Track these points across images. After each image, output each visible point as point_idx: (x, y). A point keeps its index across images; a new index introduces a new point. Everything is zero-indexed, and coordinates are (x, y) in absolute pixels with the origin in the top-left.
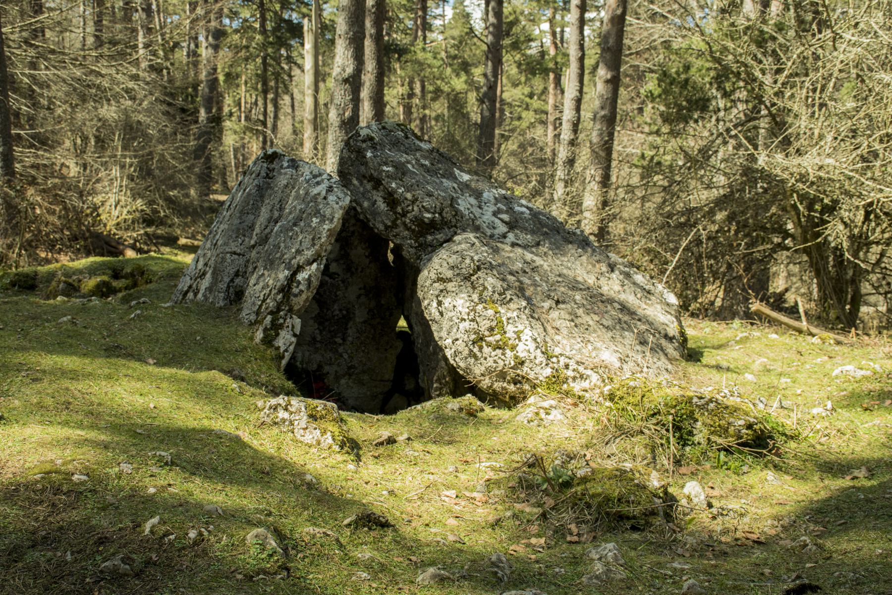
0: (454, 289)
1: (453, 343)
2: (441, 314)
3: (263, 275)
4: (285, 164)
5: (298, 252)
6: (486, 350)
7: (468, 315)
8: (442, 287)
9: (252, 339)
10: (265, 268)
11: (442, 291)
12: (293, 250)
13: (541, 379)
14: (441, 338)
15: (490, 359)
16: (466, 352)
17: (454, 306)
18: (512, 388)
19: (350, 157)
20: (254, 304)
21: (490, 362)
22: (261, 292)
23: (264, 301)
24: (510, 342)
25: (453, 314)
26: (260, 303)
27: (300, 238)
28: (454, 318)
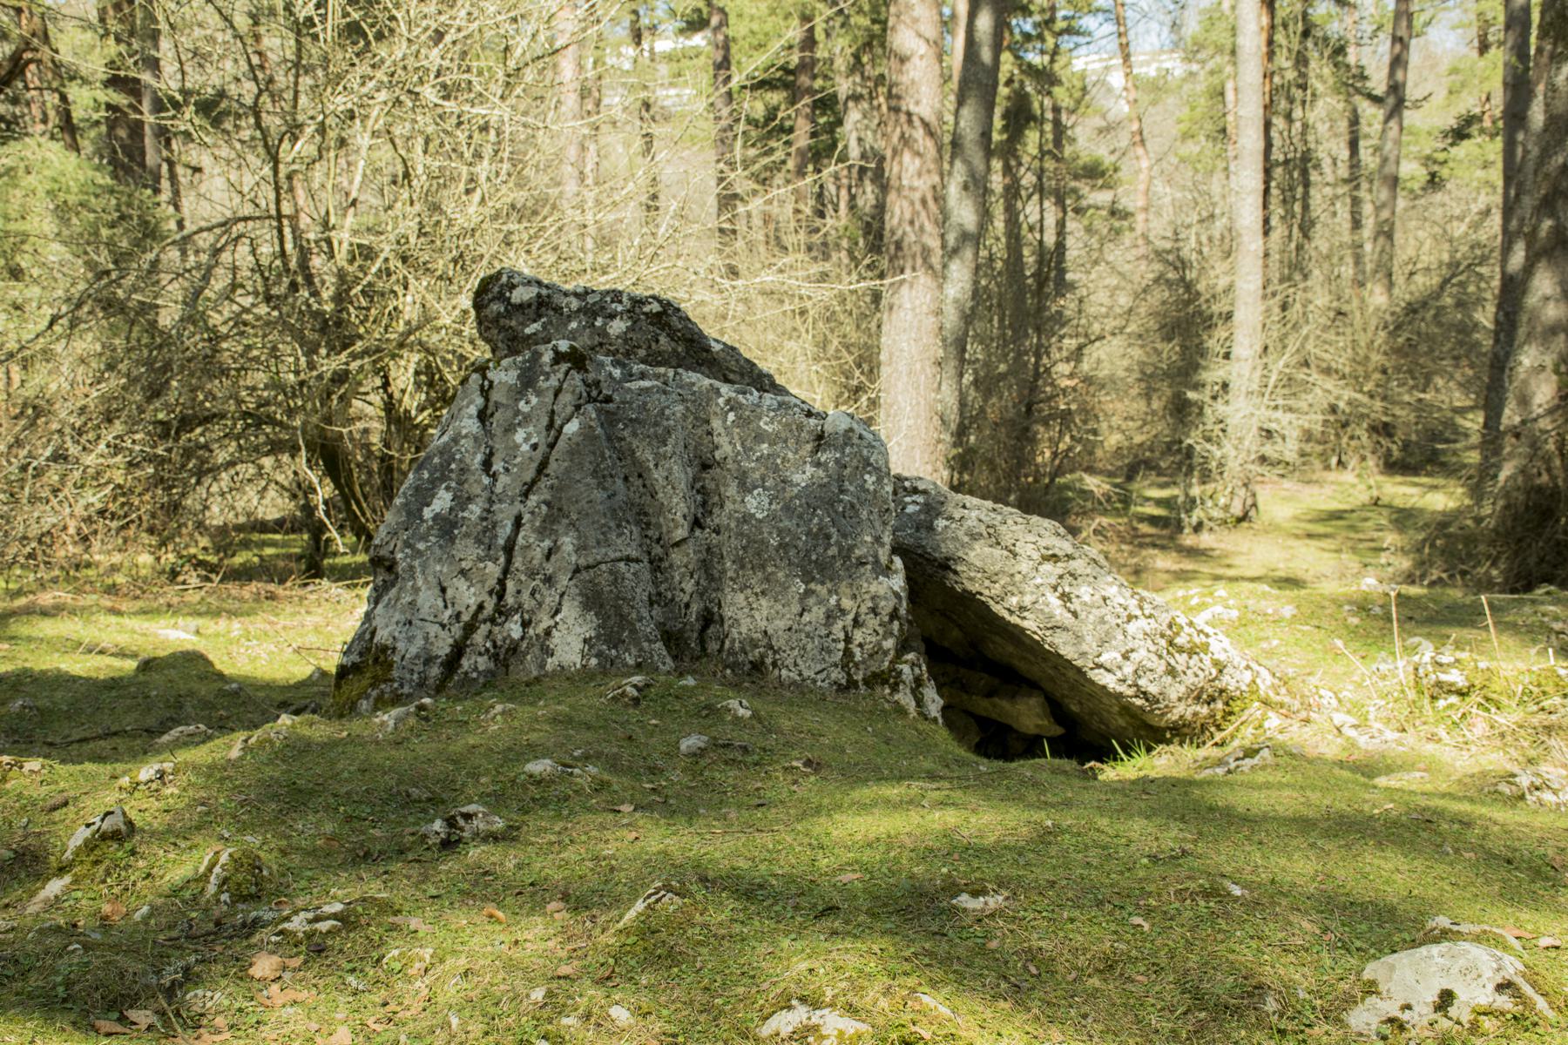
0: (1088, 571)
1: (1126, 657)
2: (1075, 614)
3: (809, 593)
4: (617, 373)
5: (878, 540)
6: (1182, 658)
7: (1141, 608)
8: (1061, 571)
9: (901, 711)
10: (808, 578)
11: (1061, 577)
12: (868, 539)
13: (1244, 688)
14: (1083, 654)
15: (1196, 672)
16: (1161, 667)
18: (1204, 710)
19: (674, 350)
21: (1190, 679)
23: (848, 640)
24: (1197, 640)
25: (1103, 611)
26: (841, 645)
27: (864, 514)
28: (1108, 618)
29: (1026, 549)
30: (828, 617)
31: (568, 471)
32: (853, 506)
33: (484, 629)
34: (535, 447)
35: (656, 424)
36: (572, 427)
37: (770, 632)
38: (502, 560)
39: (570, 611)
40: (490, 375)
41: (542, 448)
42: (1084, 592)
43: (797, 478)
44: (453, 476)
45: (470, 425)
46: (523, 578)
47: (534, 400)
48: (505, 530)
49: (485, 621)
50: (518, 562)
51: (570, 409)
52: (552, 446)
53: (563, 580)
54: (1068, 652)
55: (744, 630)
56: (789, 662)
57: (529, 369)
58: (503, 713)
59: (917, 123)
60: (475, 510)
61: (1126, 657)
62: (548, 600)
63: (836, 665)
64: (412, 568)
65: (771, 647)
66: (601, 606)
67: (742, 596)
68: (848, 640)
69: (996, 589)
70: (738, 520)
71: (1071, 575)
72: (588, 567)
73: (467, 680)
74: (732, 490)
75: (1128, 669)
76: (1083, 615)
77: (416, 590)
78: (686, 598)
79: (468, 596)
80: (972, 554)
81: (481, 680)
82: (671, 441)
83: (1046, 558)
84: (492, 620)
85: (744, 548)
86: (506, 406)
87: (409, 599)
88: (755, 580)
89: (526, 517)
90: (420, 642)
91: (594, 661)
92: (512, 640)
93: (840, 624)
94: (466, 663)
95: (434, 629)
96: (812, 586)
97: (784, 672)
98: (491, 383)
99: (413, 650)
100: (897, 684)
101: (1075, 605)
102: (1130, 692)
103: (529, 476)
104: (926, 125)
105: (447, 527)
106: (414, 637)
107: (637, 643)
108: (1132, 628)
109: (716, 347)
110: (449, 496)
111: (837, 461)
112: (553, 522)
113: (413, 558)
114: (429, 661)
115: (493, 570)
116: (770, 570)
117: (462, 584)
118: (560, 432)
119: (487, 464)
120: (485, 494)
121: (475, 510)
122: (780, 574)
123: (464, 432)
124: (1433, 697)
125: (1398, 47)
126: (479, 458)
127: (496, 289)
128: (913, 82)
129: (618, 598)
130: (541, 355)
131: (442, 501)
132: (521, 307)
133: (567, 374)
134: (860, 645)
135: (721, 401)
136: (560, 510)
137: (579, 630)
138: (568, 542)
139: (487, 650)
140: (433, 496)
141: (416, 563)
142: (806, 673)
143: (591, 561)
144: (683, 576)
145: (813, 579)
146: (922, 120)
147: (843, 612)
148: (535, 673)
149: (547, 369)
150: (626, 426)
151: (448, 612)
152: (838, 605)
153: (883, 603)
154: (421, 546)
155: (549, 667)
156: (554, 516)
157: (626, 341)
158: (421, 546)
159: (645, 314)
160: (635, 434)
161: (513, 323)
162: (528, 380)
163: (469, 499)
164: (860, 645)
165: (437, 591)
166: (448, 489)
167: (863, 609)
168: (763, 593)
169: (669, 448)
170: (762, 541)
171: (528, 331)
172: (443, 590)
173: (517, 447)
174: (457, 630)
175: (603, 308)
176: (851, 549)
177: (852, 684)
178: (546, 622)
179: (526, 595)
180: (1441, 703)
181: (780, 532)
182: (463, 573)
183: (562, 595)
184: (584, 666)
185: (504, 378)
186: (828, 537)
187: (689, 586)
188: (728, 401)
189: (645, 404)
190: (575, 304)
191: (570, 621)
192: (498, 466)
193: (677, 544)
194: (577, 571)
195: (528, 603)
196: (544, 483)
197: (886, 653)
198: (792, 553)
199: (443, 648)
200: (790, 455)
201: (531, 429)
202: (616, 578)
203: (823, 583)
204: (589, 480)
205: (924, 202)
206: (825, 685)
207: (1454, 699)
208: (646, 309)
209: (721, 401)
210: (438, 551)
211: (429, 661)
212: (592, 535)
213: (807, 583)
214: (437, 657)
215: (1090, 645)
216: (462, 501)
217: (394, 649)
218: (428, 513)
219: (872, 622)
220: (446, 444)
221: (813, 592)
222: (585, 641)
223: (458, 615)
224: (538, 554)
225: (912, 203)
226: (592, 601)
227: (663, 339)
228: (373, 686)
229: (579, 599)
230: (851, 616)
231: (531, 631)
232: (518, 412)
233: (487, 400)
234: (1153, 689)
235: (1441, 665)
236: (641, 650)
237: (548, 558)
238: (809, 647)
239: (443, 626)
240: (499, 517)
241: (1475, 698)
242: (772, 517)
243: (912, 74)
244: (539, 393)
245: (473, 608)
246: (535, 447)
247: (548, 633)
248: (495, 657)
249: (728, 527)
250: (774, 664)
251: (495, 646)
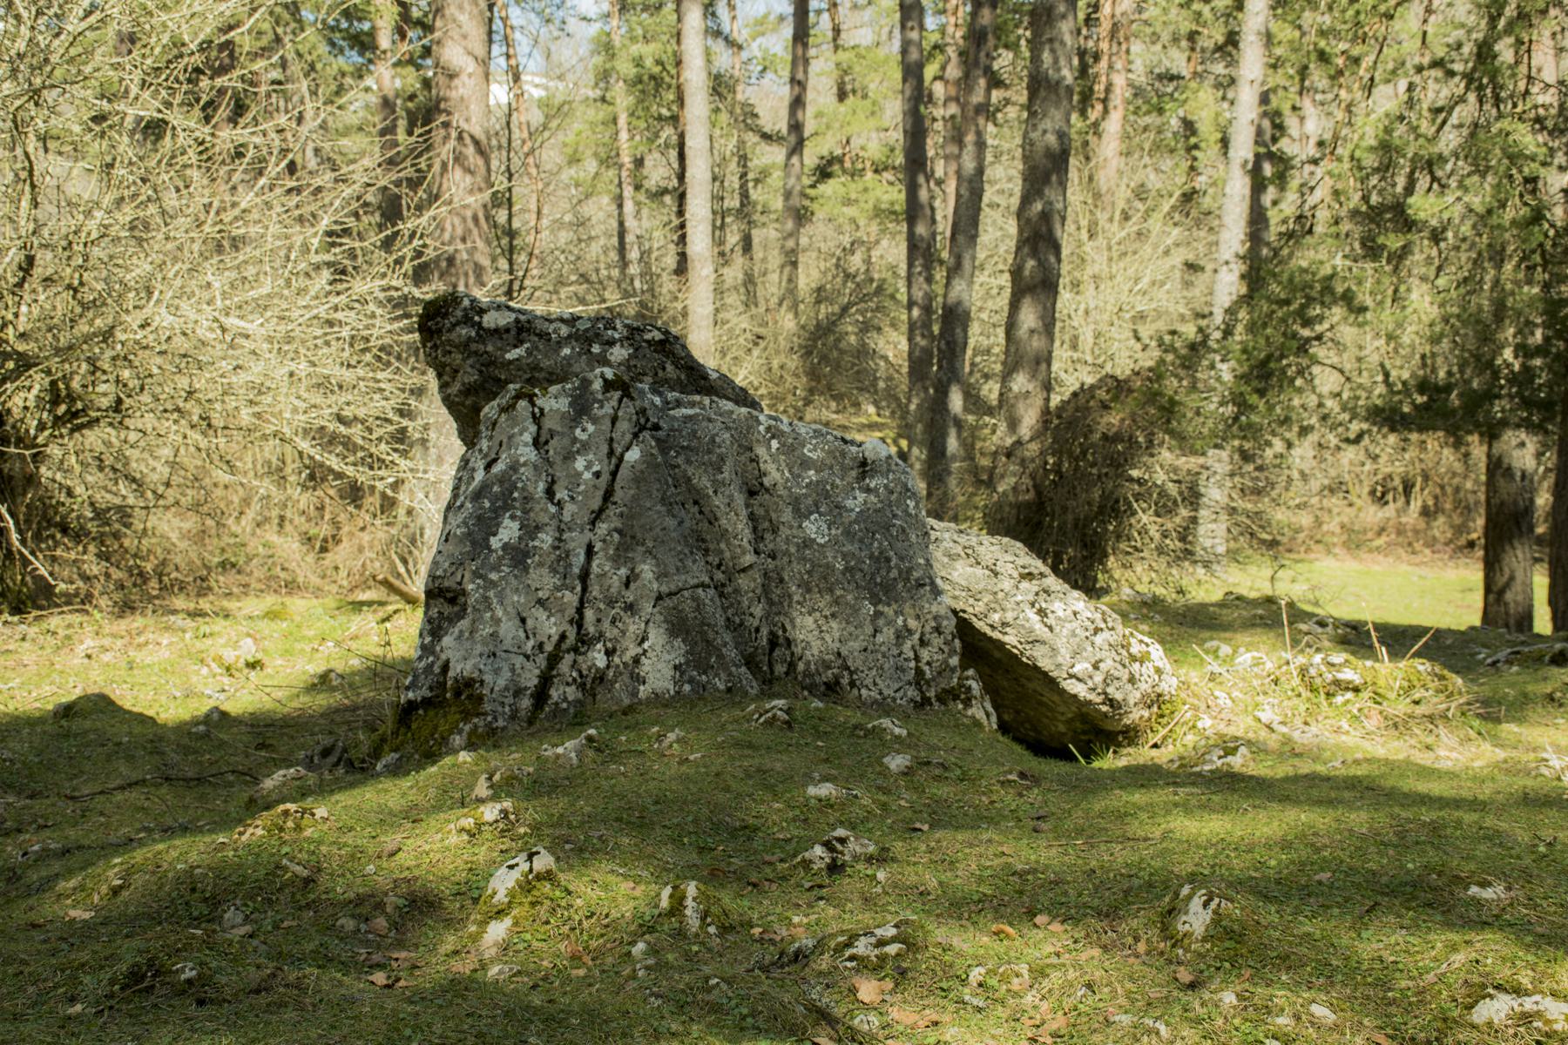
1: (1096, 667)
2: (1051, 628)
3: (878, 614)
4: (657, 400)
8: (1036, 589)
10: (875, 601)
14: (1059, 666)
17: (1075, 614)
20: (900, 669)
22: (899, 645)
25: (1075, 625)
26: (912, 664)
28: (1078, 631)
29: (1006, 568)
30: (898, 637)
31: (635, 498)
32: (904, 530)
33: (568, 658)
34: (597, 475)
35: (709, 452)
36: (633, 455)
37: (844, 652)
38: (579, 588)
39: (656, 637)
40: (539, 402)
41: (606, 477)
42: (1057, 607)
43: (849, 503)
44: (517, 504)
45: (527, 453)
46: (602, 606)
47: (591, 428)
48: (579, 559)
49: (568, 651)
50: (595, 591)
51: (628, 437)
52: (614, 474)
53: (647, 608)
54: (1045, 664)
55: (816, 653)
56: (869, 681)
57: (580, 396)
58: (678, 741)
59: (468, 140)
60: (545, 539)
61: (1096, 667)
62: (632, 628)
63: (910, 683)
64: (486, 599)
65: (848, 668)
66: (688, 632)
67: (809, 621)
68: (917, 658)
69: (980, 607)
70: (798, 545)
71: (1045, 591)
72: (670, 594)
73: (557, 711)
74: (787, 515)
75: (1098, 678)
76: (1057, 629)
77: (498, 621)
78: (756, 623)
79: (550, 627)
80: (956, 574)
81: (572, 710)
82: (726, 468)
83: (1023, 577)
84: (575, 650)
85: (808, 572)
86: (562, 434)
87: (489, 630)
88: (823, 602)
89: (598, 546)
90: (506, 674)
91: (687, 687)
92: (598, 669)
93: (908, 644)
94: (555, 694)
95: (519, 661)
96: (880, 607)
97: (864, 692)
98: (542, 410)
99: (502, 682)
100: (969, 699)
101: (1051, 621)
102: (1099, 699)
103: (596, 503)
104: (477, 143)
105: (519, 556)
106: (499, 669)
107: (726, 669)
108: (1098, 639)
109: (714, 375)
110: (516, 525)
111: (886, 486)
112: (626, 550)
113: (486, 588)
114: (518, 692)
115: (570, 598)
116: (839, 593)
117: (541, 614)
118: (621, 459)
119: (550, 493)
120: (554, 523)
121: (545, 539)
122: (849, 597)
123: (522, 460)
124: (1328, 694)
125: (797, 88)
126: (541, 486)
127: (459, 313)
128: (462, 99)
129: (703, 624)
130: (590, 383)
131: (509, 531)
132: (496, 331)
133: (620, 401)
134: (928, 663)
135: (761, 428)
136: (633, 537)
137: (667, 657)
138: (647, 570)
139: (575, 680)
140: (498, 525)
141: (491, 594)
142: (886, 692)
143: (673, 588)
144: (751, 601)
145: (880, 601)
146: (472, 137)
147: (910, 632)
148: (627, 702)
149: (600, 397)
150: (678, 453)
151: (531, 643)
152: (905, 625)
153: (945, 623)
154: (494, 576)
155: (641, 695)
156: (627, 544)
157: (629, 368)
158: (494, 576)
159: (648, 342)
160: (689, 462)
161: (490, 348)
162: (581, 407)
163: (538, 528)
164: (928, 663)
165: (517, 622)
166: (513, 517)
167: (928, 629)
168: (833, 615)
169: (726, 475)
170: (828, 566)
171: (508, 356)
172: (523, 621)
173: (579, 475)
174: (541, 660)
175: (597, 335)
176: (909, 571)
177: (926, 701)
178: (633, 651)
179: (606, 624)
180: (1339, 699)
181: (844, 556)
182: (540, 602)
183: (647, 623)
184: (678, 693)
185: (556, 406)
186: (888, 560)
187: (758, 610)
188: (768, 429)
189: (694, 432)
190: (564, 331)
191: (658, 648)
192: (561, 494)
193: (744, 570)
194: (659, 598)
195: (611, 632)
196: (612, 511)
197: (953, 670)
198: (858, 576)
199: (530, 679)
200: (838, 481)
201: (591, 457)
202: (699, 606)
203: (889, 605)
204: (659, 507)
205: (475, 219)
206: (903, 702)
207: (1349, 695)
208: (648, 336)
209: (761, 428)
210: (514, 582)
211: (518, 692)
212: (672, 563)
213: (875, 605)
214: (526, 688)
215: (1064, 656)
216: (530, 530)
217: (482, 682)
218: (495, 543)
219: (937, 641)
220: (504, 473)
221: (882, 613)
222: (676, 667)
223: (541, 646)
224: (615, 582)
225: (464, 220)
226: (677, 627)
227: (669, 367)
228: (466, 720)
229: (665, 626)
230: (917, 636)
231: (617, 660)
232: (575, 440)
233: (540, 428)
234: (1118, 696)
235: (1333, 665)
236: (730, 674)
237: (627, 585)
238: (886, 666)
239: (527, 657)
240: (571, 545)
241: (1365, 695)
242: (834, 542)
243: (461, 91)
244: (595, 421)
245: (555, 638)
246: (597, 475)
247: (636, 661)
248: (582, 686)
249: (787, 553)
250: (852, 684)
251: (581, 676)
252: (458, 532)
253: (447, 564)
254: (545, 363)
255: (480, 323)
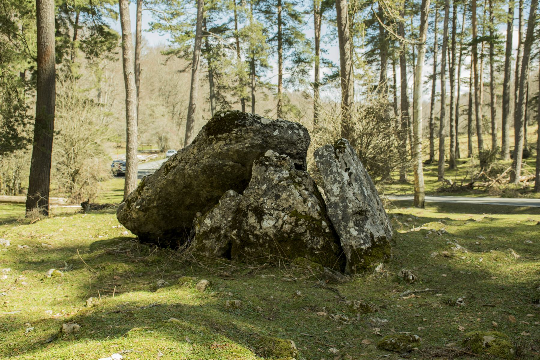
132: (266, 125)
161: (268, 131)
252: (359, 192)
253: (361, 203)
254: (285, 136)
255: (261, 122)
